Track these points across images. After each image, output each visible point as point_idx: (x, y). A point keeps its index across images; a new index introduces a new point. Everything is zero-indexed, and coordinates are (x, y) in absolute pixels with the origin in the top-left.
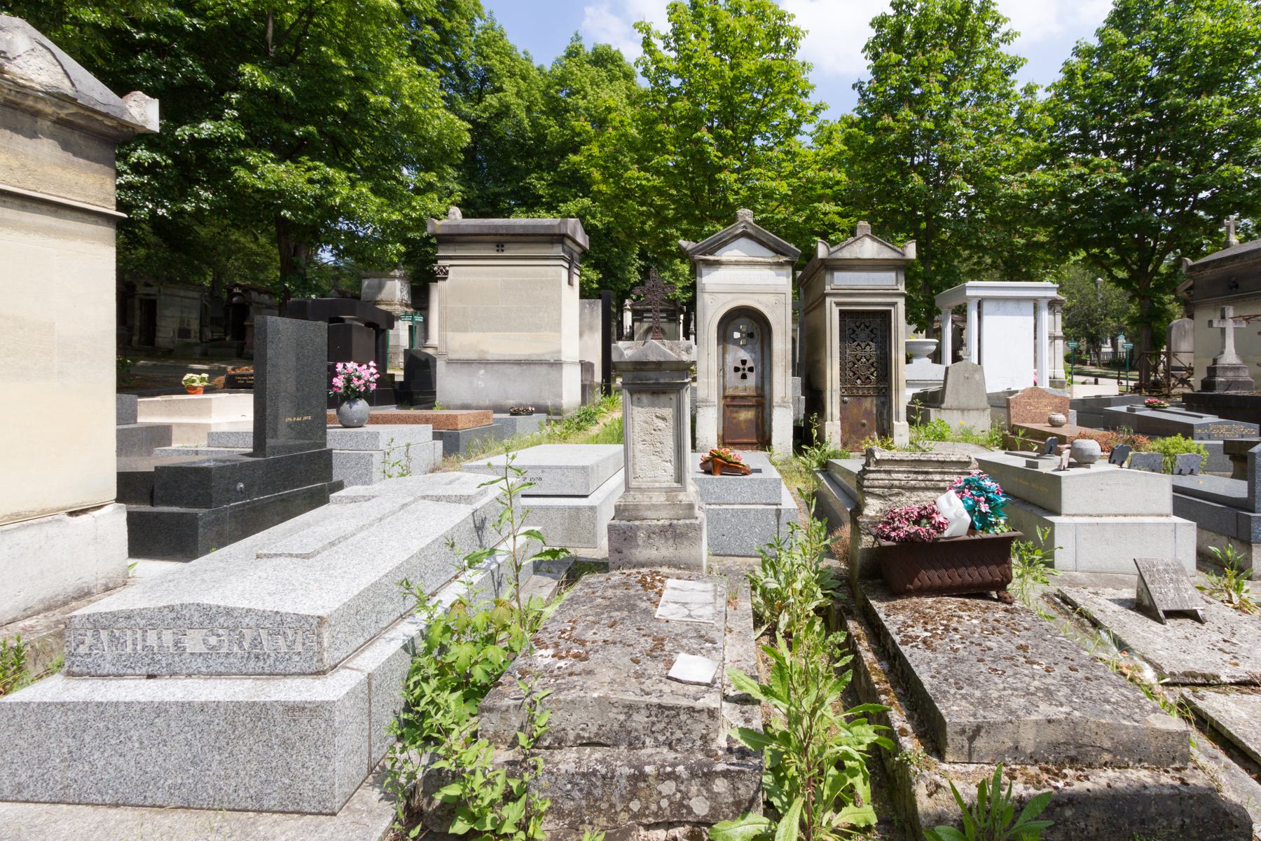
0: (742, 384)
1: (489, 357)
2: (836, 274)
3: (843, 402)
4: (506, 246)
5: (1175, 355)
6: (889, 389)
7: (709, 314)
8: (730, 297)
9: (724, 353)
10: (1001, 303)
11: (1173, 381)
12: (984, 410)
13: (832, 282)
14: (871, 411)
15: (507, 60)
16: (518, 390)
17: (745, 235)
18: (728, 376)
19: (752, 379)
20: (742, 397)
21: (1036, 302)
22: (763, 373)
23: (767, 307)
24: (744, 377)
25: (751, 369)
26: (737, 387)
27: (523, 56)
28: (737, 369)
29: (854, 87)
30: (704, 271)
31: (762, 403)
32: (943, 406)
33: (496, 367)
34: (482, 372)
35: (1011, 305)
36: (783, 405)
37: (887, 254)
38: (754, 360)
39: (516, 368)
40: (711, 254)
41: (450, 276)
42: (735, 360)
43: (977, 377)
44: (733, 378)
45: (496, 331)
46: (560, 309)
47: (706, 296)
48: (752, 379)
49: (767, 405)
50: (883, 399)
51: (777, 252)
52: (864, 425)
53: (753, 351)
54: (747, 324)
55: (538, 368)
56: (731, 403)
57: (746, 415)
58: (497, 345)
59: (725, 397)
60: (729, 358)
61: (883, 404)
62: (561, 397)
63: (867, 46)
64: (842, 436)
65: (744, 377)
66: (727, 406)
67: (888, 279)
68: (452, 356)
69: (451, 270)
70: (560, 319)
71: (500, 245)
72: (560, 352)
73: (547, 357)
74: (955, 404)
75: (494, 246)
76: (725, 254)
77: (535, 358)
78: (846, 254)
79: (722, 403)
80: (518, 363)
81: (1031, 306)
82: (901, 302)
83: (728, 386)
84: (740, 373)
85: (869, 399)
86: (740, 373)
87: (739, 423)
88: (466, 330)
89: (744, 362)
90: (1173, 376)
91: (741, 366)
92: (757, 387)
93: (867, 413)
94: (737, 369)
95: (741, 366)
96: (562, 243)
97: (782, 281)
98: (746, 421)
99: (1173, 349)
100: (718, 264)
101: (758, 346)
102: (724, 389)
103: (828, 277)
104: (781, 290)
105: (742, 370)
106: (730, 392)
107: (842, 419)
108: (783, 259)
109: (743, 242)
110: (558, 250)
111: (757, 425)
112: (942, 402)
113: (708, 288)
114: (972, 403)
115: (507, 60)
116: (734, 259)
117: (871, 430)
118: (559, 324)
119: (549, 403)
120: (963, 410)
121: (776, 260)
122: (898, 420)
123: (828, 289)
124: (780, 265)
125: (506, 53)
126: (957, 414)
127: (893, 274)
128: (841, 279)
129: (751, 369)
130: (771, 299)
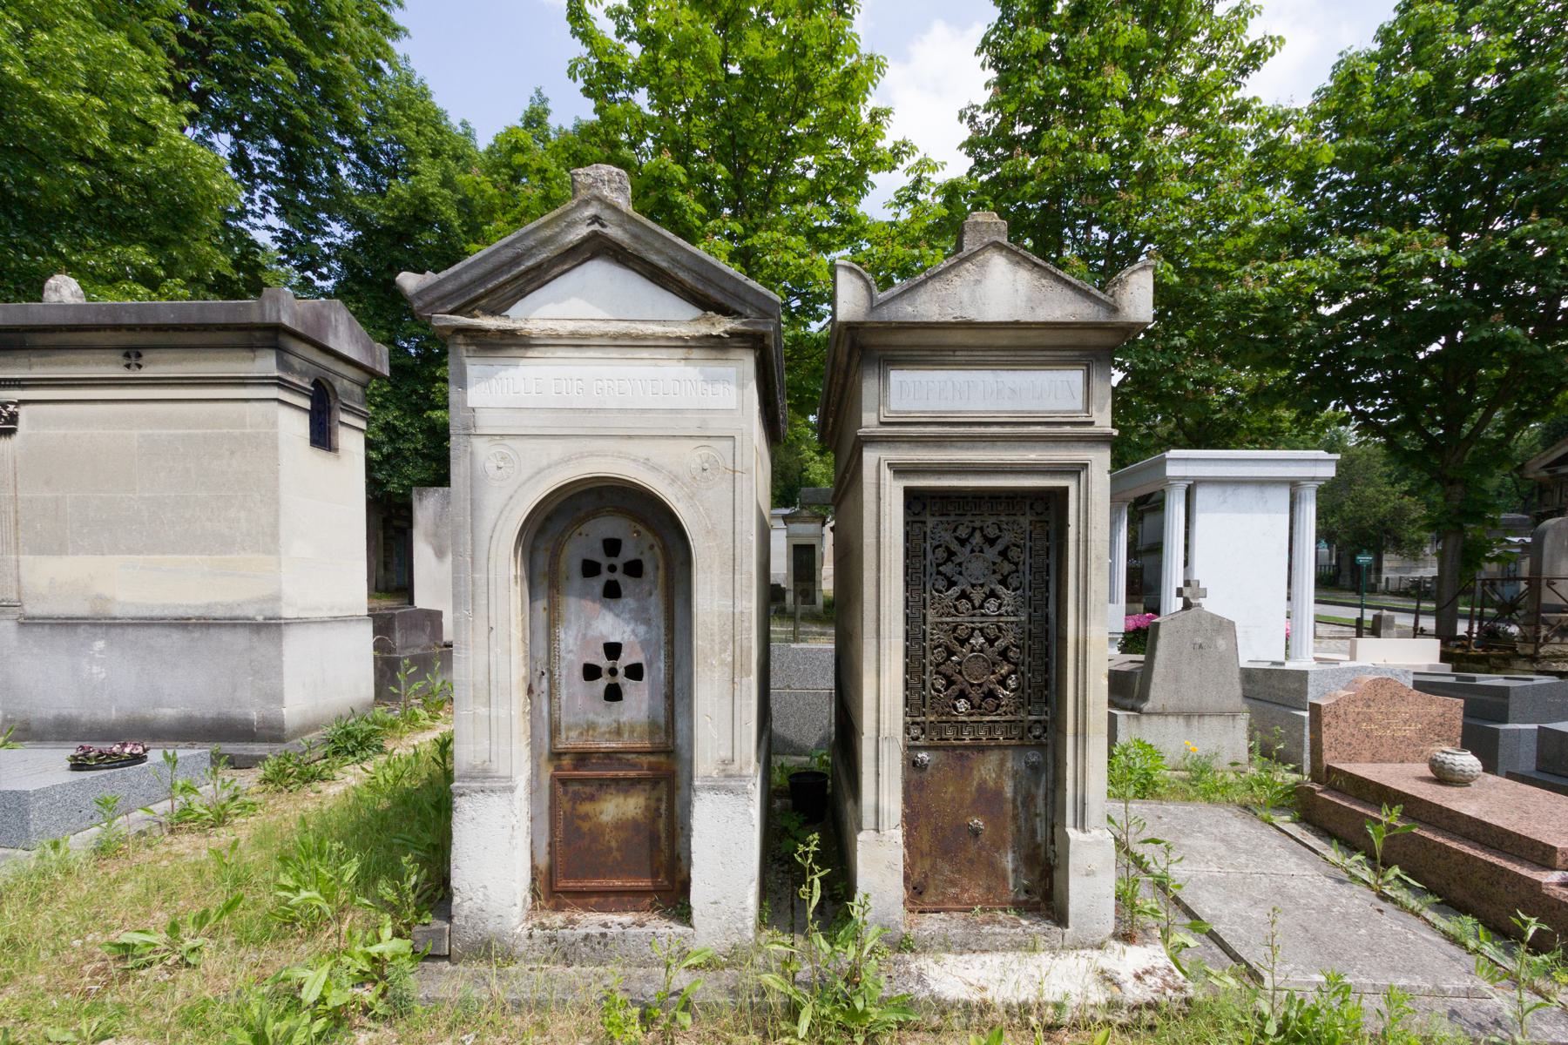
0: (606, 716)
1: (117, 611)
2: (897, 377)
3: (912, 765)
4: (147, 356)
5: (1550, 584)
6: (1055, 726)
7: (492, 501)
8: (557, 449)
9: (553, 622)
10: (1229, 490)
11: (1544, 632)
12: (1234, 715)
13: (882, 398)
14: (998, 793)
15: (429, 130)
16: (184, 685)
17: (598, 248)
18: (564, 693)
19: (639, 702)
20: (609, 755)
21: (1294, 485)
22: (671, 682)
23: (674, 479)
24: (613, 694)
25: (635, 672)
26: (591, 726)
27: (460, 130)
28: (591, 672)
29: (961, 119)
30: (475, 368)
31: (664, 770)
32: (1147, 707)
33: (131, 633)
34: (100, 645)
35: (1247, 494)
36: (727, 783)
37: (1062, 307)
38: (645, 645)
39: (177, 636)
40: (494, 312)
41: (22, 425)
42: (585, 641)
43: (1221, 643)
44: (580, 700)
45: (131, 551)
46: (277, 501)
47: (480, 445)
48: (639, 702)
49: (682, 779)
50: (1034, 757)
51: (704, 303)
52: (976, 833)
53: (640, 616)
54: (605, 537)
55: (227, 636)
56: (572, 774)
57: (618, 808)
58: (133, 583)
59: (556, 755)
60: (568, 638)
61: (1035, 769)
62: (278, 699)
63: (985, 41)
64: (909, 867)
65: (613, 694)
66: (561, 782)
67: (1056, 391)
68: (33, 609)
69: (23, 412)
70: (275, 526)
71: (133, 354)
72: (277, 598)
73: (250, 611)
74: (1171, 703)
75: (118, 356)
76: (536, 312)
77: (219, 613)
78: (928, 306)
79: (547, 772)
80: (182, 624)
81: (1284, 495)
82: (1100, 461)
83: (565, 720)
84: (602, 684)
85: (993, 758)
86: (602, 684)
87: (598, 832)
88: (61, 550)
89: (613, 650)
90: (1545, 622)
91: (604, 663)
92: (653, 726)
93: (988, 799)
94: (591, 672)
95: (604, 663)
96: (280, 349)
97: (728, 393)
98: (620, 825)
99: (1546, 572)
100: (513, 342)
101: (656, 604)
102: (554, 731)
103: (869, 387)
104: (717, 426)
105: (608, 674)
106: (571, 740)
107: (911, 820)
108: (723, 326)
109: (598, 273)
110: (266, 364)
111: (654, 838)
112: (1144, 696)
113: (486, 423)
114: (1210, 700)
115: (429, 130)
116: (566, 327)
117: (997, 846)
118: (275, 536)
119: (254, 715)
120: (1188, 716)
121: (704, 329)
122: (1081, 824)
123: (869, 421)
124: (715, 345)
125: (435, 119)
126: (1175, 725)
127: (1075, 377)
128: (909, 393)
129: (635, 672)
130: (689, 455)
